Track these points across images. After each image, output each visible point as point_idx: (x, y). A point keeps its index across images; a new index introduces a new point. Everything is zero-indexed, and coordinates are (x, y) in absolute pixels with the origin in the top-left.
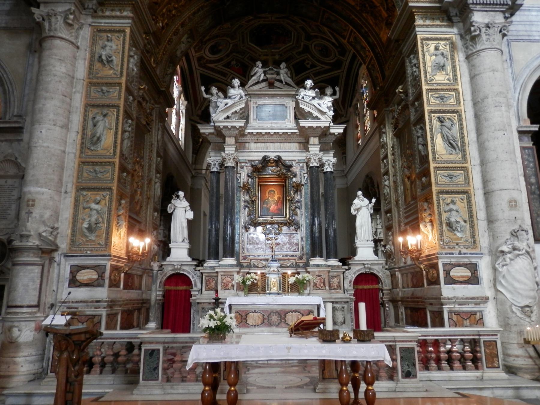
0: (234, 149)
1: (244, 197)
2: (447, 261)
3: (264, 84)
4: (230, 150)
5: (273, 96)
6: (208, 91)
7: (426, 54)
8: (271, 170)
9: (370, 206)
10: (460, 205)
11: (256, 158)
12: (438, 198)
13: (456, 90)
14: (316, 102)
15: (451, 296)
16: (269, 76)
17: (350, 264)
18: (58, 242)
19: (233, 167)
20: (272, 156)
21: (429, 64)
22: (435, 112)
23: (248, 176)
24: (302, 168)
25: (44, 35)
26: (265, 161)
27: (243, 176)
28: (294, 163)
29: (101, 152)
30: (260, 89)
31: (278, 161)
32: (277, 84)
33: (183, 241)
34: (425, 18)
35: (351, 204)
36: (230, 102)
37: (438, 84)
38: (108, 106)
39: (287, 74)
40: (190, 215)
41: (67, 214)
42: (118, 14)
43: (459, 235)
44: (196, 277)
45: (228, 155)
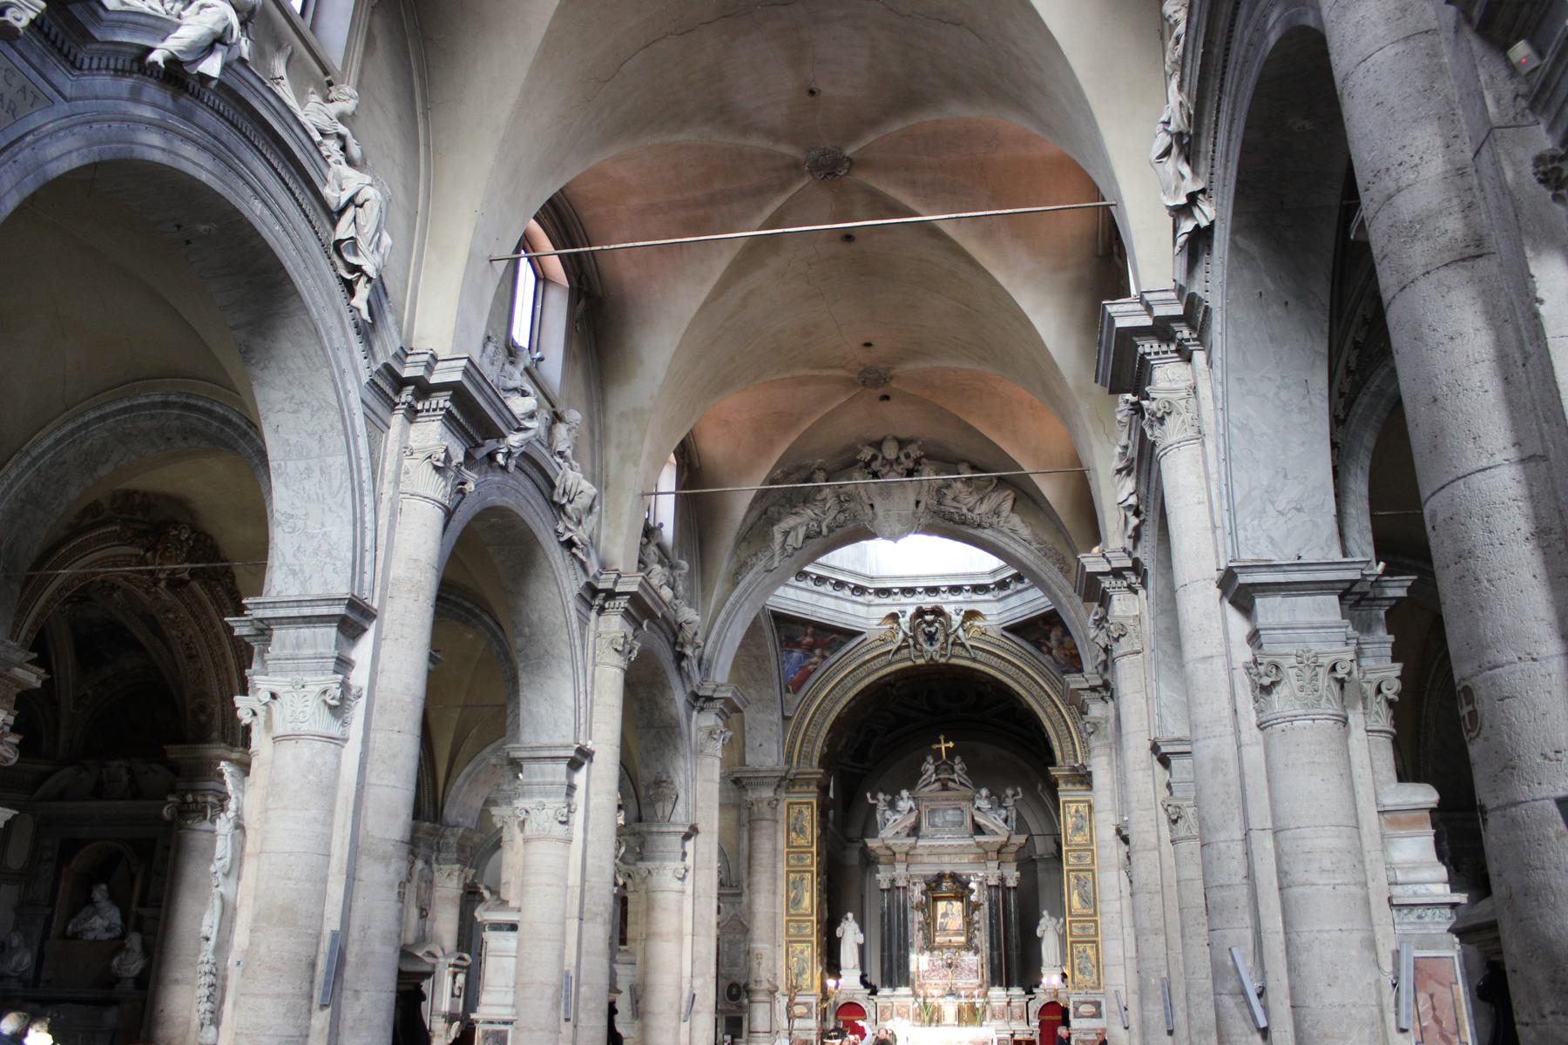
0: (905, 867)
1: (918, 917)
2: (1077, 999)
3: (937, 785)
4: (900, 869)
5: (947, 799)
6: (874, 797)
7: (1068, 816)
8: (946, 885)
9: (1058, 926)
10: (1091, 952)
11: (929, 873)
12: (1071, 946)
13: (1092, 850)
14: (991, 815)
15: (1077, 1027)
16: (941, 776)
17: (1032, 993)
18: (778, 983)
19: (904, 888)
20: (948, 870)
21: (1069, 825)
22: (1073, 871)
23: (922, 893)
24: (981, 883)
25: (753, 818)
26: (940, 877)
27: (917, 893)
28: (972, 878)
29: (801, 911)
30: (931, 791)
31: (954, 877)
32: (951, 784)
33: (854, 968)
34: (1066, 783)
35: (1037, 924)
36: (897, 816)
37: (1076, 845)
38: (804, 871)
39: (961, 770)
40: (860, 938)
41: (782, 963)
42: (805, 788)
43: (1087, 978)
44: (869, 1007)
45: (899, 875)
